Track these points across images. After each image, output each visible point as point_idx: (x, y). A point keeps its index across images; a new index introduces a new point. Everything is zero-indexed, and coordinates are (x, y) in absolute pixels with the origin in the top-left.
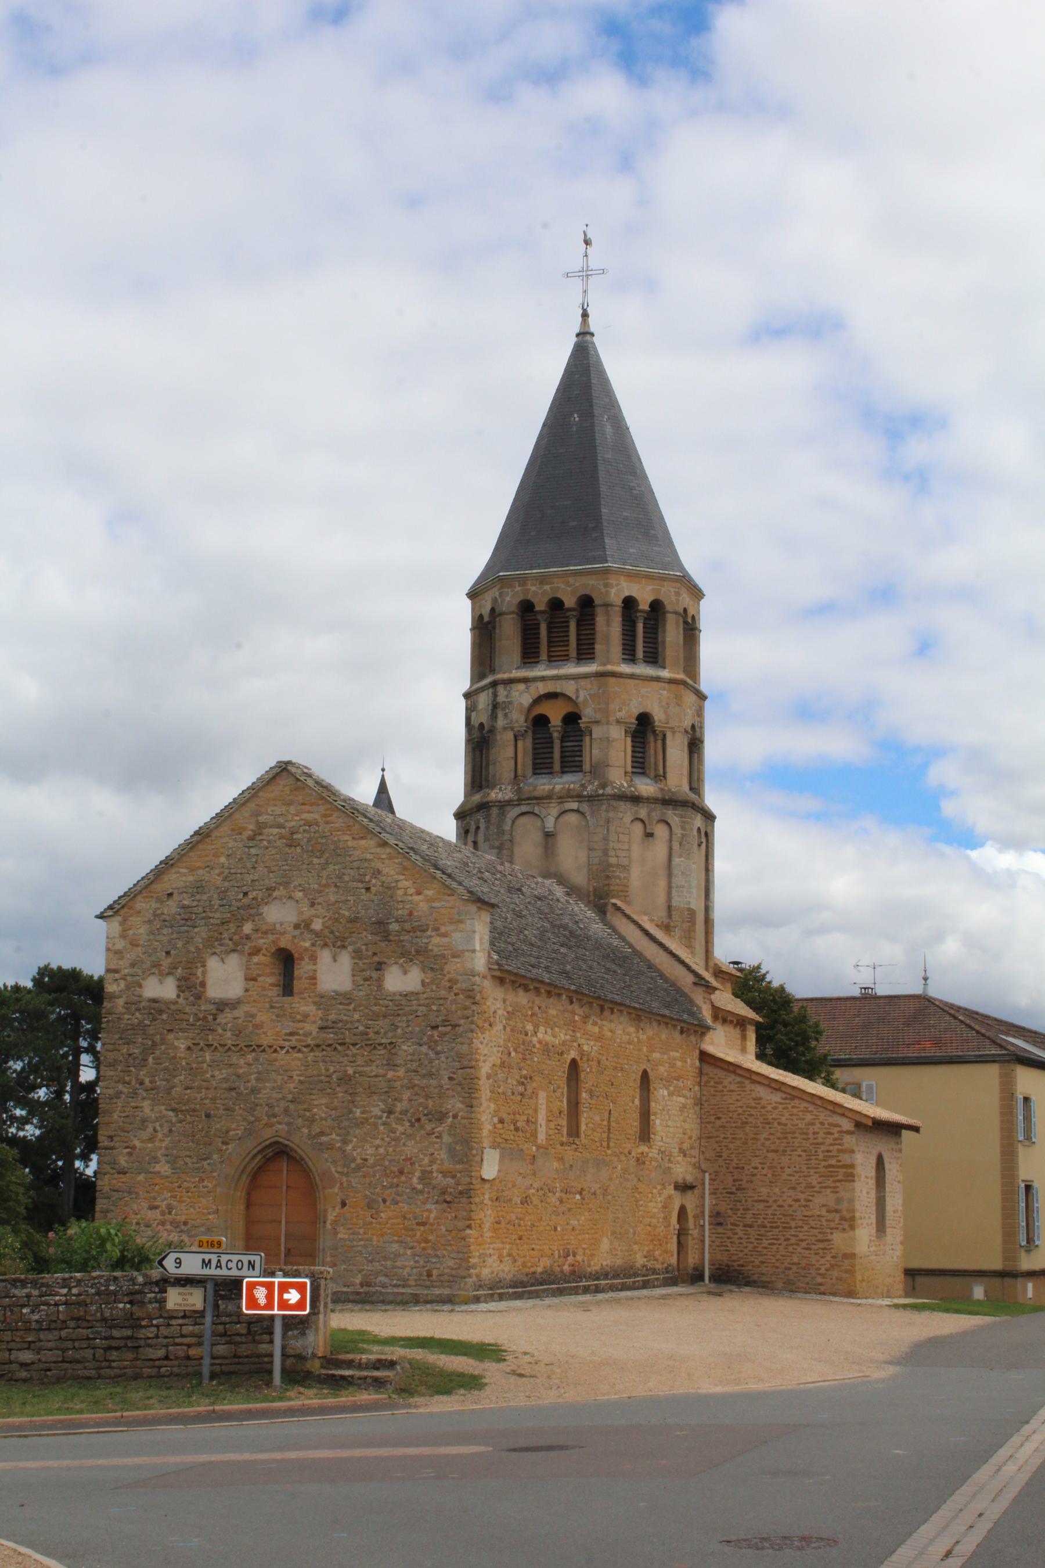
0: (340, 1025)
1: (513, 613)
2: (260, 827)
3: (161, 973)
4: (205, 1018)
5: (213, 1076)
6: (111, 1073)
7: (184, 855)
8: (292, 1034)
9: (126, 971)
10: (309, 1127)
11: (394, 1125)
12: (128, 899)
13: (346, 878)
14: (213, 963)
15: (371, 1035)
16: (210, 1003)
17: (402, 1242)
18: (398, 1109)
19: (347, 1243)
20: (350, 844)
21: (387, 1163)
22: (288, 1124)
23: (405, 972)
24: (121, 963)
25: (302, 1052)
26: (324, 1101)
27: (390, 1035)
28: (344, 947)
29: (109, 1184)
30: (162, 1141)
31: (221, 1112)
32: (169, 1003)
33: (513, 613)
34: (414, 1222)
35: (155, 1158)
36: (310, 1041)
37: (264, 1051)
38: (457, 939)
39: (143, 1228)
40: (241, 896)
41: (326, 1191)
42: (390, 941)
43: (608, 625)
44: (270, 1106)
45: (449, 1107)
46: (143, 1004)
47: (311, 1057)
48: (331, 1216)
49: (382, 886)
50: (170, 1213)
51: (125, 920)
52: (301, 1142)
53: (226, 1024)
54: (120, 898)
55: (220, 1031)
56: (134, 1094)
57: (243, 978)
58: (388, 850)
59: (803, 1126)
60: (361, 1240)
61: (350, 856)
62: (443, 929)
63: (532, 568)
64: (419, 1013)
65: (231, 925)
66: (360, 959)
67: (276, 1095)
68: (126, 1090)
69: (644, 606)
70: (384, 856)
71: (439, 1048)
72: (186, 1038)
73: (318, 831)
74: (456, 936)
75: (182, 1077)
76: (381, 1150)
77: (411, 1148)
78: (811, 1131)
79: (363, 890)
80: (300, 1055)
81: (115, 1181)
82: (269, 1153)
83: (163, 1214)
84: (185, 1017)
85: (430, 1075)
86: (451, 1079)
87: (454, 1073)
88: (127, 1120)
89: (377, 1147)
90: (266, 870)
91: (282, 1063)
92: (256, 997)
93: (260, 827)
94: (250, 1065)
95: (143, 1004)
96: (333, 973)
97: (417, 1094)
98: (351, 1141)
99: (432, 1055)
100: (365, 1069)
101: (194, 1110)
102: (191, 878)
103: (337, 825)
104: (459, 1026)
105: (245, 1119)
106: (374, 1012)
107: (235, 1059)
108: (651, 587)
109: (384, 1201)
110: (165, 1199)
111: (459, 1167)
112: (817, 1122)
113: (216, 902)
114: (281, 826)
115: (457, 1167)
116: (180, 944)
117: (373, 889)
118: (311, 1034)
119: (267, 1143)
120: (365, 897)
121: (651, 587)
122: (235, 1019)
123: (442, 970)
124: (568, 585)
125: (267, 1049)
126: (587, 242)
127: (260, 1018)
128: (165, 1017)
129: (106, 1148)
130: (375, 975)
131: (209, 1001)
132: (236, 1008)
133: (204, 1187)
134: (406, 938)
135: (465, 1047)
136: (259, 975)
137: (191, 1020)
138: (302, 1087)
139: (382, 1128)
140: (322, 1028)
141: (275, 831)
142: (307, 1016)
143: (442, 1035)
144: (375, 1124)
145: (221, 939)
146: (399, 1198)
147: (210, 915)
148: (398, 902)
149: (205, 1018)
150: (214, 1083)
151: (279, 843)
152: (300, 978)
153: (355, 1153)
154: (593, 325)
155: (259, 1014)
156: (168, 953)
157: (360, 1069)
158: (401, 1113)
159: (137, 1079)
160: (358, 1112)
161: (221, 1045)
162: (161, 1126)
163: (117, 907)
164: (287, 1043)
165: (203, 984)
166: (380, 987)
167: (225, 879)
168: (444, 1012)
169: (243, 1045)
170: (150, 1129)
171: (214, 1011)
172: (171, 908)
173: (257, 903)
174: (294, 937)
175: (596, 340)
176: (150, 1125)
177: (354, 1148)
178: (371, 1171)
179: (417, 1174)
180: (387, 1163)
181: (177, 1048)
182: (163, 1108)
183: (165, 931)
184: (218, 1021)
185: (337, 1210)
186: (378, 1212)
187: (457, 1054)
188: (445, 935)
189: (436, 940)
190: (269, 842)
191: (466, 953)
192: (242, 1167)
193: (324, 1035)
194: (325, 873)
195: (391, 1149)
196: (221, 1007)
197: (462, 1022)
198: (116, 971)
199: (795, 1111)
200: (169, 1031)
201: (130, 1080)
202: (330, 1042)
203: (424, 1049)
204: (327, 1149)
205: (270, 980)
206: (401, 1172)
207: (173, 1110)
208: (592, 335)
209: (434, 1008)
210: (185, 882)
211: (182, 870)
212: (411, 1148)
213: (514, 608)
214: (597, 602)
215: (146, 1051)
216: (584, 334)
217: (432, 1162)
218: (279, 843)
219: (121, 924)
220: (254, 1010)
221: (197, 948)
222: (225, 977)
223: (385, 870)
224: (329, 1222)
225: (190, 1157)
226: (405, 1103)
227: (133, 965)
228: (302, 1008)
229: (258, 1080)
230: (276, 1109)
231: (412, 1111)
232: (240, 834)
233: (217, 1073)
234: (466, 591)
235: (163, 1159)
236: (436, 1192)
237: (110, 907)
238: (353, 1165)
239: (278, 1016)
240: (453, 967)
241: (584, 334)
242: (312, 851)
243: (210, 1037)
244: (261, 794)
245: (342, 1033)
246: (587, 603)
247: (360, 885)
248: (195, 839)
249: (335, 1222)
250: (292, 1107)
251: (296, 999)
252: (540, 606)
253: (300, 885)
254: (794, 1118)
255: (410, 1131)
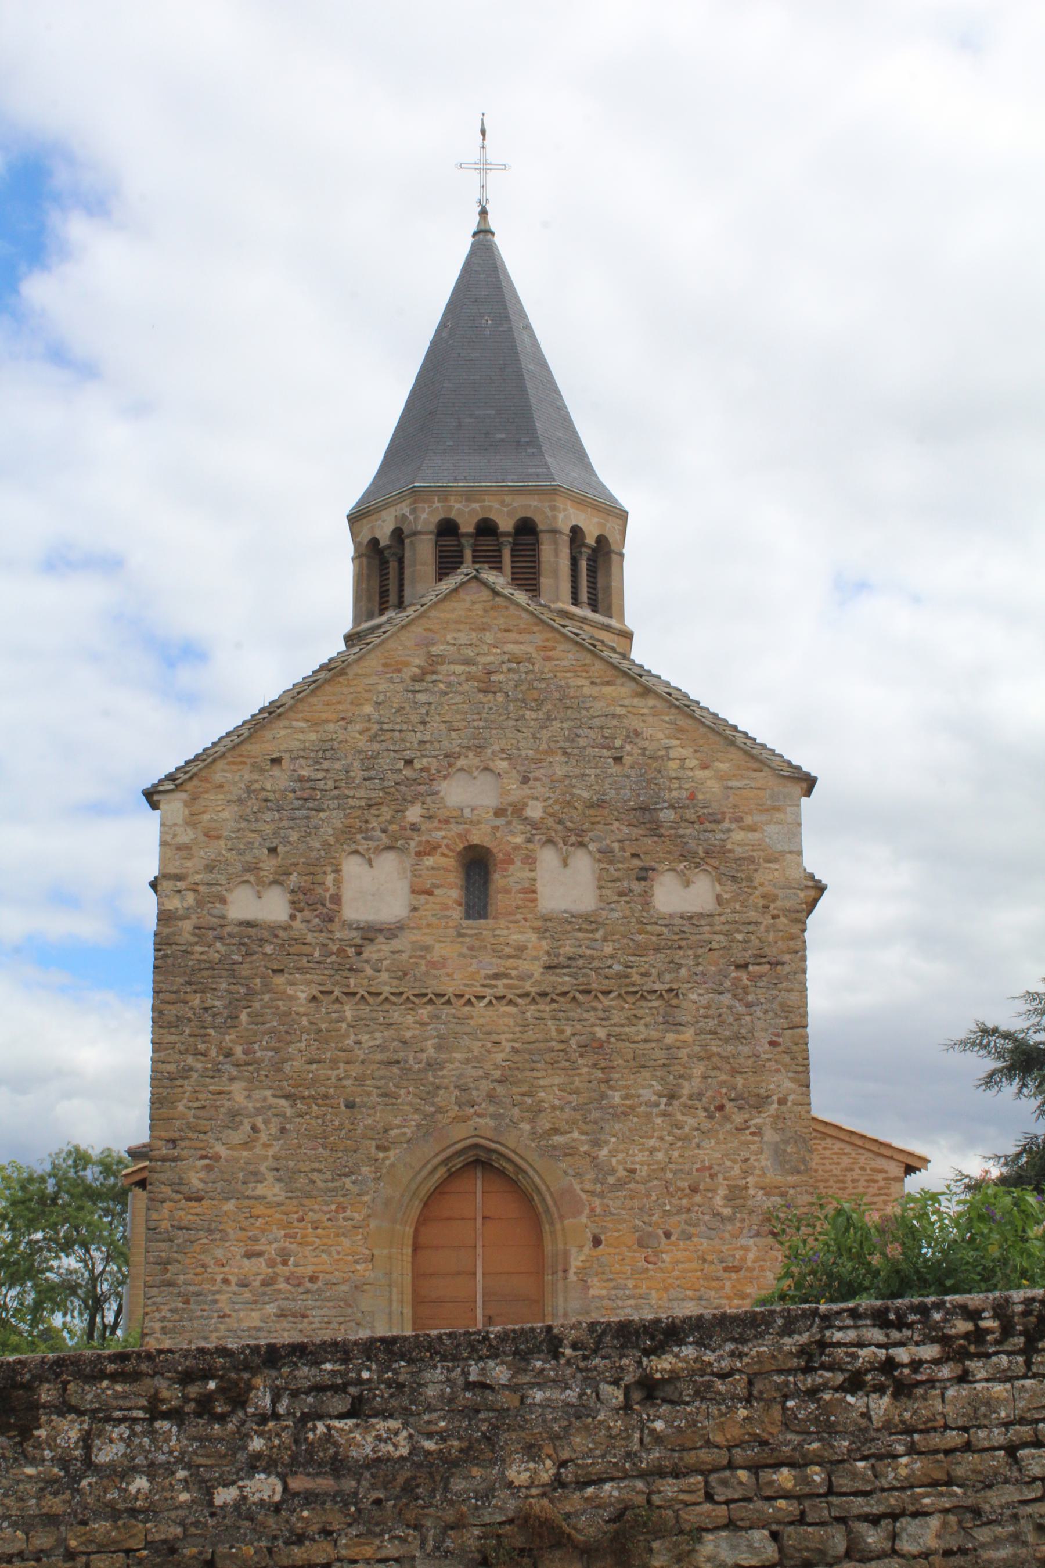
0: (580, 962)
1: (431, 533)
2: (433, 663)
3: (260, 882)
4: (341, 951)
5: (358, 1043)
6: (173, 1039)
7: (301, 700)
8: (497, 976)
9: (198, 878)
10: (532, 1121)
11: (679, 1117)
12: (202, 765)
13: (582, 742)
14: (352, 867)
15: (635, 978)
16: (351, 928)
17: (700, 1299)
18: (685, 1092)
19: (606, 1302)
20: (587, 691)
21: (670, 1175)
22: (494, 1116)
23: (687, 884)
24: (189, 864)
25: (516, 1005)
26: (557, 1080)
27: (667, 977)
28: (582, 845)
29: (172, 1218)
30: (265, 1146)
31: (374, 1098)
32: (274, 929)
33: (431, 533)
34: (720, 1267)
35: (255, 1174)
36: (528, 987)
37: (448, 1002)
38: (772, 834)
39: (235, 1288)
40: (401, 764)
41: (566, 1222)
42: (660, 836)
43: (557, 555)
44: (464, 1089)
45: (772, 1086)
46: (228, 929)
47: (531, 1011)
48: (576, 1261)
49: (644, 755)
50: (285, 1263)
51: (194, 798)
52: (518, 1141)
53: (380, 960)
54: (187, 763)
55: (369, 971)
56: (217, 1071)
57: (407, 890)
58: (651, 702)
59: (839, 1173)
60: (629, 1297)
61: (587, 709)
62: (748, 820)
63: (456, 480)
64: (714, 945)
65: (384, 809)
66: (611, 863)
67: (470, 1071)
68: (199, 1066)
69: (590, 541)
70: (645, 711)
71: (751, 998)
72: (308, 983)
73: (532, 671)
74: (772, 829)
75: (303, 1045)
76: (660, 1156)
77: (710, 1151)
78: (849, 1178)
79: (610, 760)
80: (512, 1009)
81: (182, 1213)
82: (458, 1163)
83: (271, 1264)
84: (306, 949)
85: (738, 1037)
86: (772, 1043)
87: (778, 1035)
88: (200, 1113)
89: (652, 1151)
90: (443, 726)
91: (481, 1021)
92: (433, 920)
93: (433, 663)
94: (423, 1024)
95: (228, 929)
96: (566, 884)
97: (715, 1068)
98: (607, 1142)
99: (741, 1009)
100: (627, 1029)
101: (326, 1097)
102: (313, 736)
103: (565, 663)
104: (783, 964)
105: (417, 1110)
106: (638, 945)
107: (396, 1016)
108: (596, 520)
109: (668, 1235)
110: (276, 1240)
111: (791, 1179)
112: (856, 1167)
113: (358, 774)
114: (467, 662)
115: (789, 1178)
116: (294, 836)
117: (627, 760)
118: (531, 976)
119: (459, 1146)
120: (615, 769)
121: (596, 520)
122: (393, 952)
123: (750, 879)
124: (503, 503)
125: (453, 1000)
126: (483, 132)
127: (439, 951)
128: (268, 949)
129: (164, 1159)
130: (637, 887)
131: (347, 925)
132: (396, 936)
133: (345, 1219)
134: (688, 831)
135: (794, 997)
136: (438, 886)
137: (317, 954)
138: (516, 1058)
139: (659, 1121)
140: (549, 968)
141: (459, 669)
142: (522, 948)
143: (755, 978)
144: (648, 1115)
145: (367, 830)
146: (692, 1230)
147: (350, 793)
148: (671, 779)
149: (341, 951)
150: (360, 1054)
151: (466, 687)
152: (507, 891)
153: (614, 1161)
154: (493, 223)
155: (437, 946)
156: (273, 850)
157: (618, 1030)
158: (690, 1098)
159: (220, 1049)
160: (616, 1098)
161: (369, 993)
162: (266, 1122)
163: (183, 777)
164: (488, 991)
165: (336, 899)
166: (647, 904)
167: (372, 739)
168: (756, 942)
169: (409, 993)
170: (247, 1127)
171: (358, 941)
172: (279, 780)
173: (428, 777)
174: (496, 828)
175: (498, 240)
176: (246, 1121)
177: (612, 1154)
178: (642, 1188)
179: (722, 1192)
180: (670, 1175)
181: (292, 998)
182: (268, 1093)
183: (268, 816)
184: (365, 956)
185: (586, 1250)
186: (656, 1253)
187: (782, 1005)
188: (752, 829)
189: (738, 836)
190: (449, 685)
191: (788, 856)
192: (414, 1186)
193: (553, 978)
194: (545, 734)
195: (676, 1154)
196: (371, 935)
197: (786, 958)
198: (179, 878)
199: (827, 1153)
200: (274, 971)
201: (208, 1049)
202: (565, 989)
203: (726, 999)
204: (566, 1155)
205: (451, 893)
206: (694, 1190)
207: (287, 1097)
208: (493, 234)
209: (739, 937)
210: (304, 741)
211: (294, 723)
212: (710, 1151)
213: (432, 527)
214: (541, 527)
215: (234, 1005)
216: (483, 233)
217: (746, 1173)
218: (466, 687)
219: (186, 805)
220: (428, 940)
221: (326, 843)
222: (374, 889)
223: (648, 732)
224: (572, 1271)
225: (320, 1171)
226: (696, 1082)
227: (210, 868)
228: (514, 937)
229: (439, 1048)
230: (475, 1093)
231: (709, 1093)
232: (399, 671)
233: (365, 1038)
234: (347, 512)
235: (270, 1176)
236: (756, 1219)
237: (171, 777)
238: (611, 1180)
239: (471, 948)
240: (766, 877)
241: (483, 233)
242: (524, 701)
243: (352, 981)
244: (433, 613)
245: (585, 975)
246: (526, 529)
247: (605, 753)
248: (322, 675)
249: (584, 1273)
250: (500, 1090)
251: (502, 923)
252: (467, 527)
253: (503, 750)
254: (827, 1162)
255: (706, 1125)
